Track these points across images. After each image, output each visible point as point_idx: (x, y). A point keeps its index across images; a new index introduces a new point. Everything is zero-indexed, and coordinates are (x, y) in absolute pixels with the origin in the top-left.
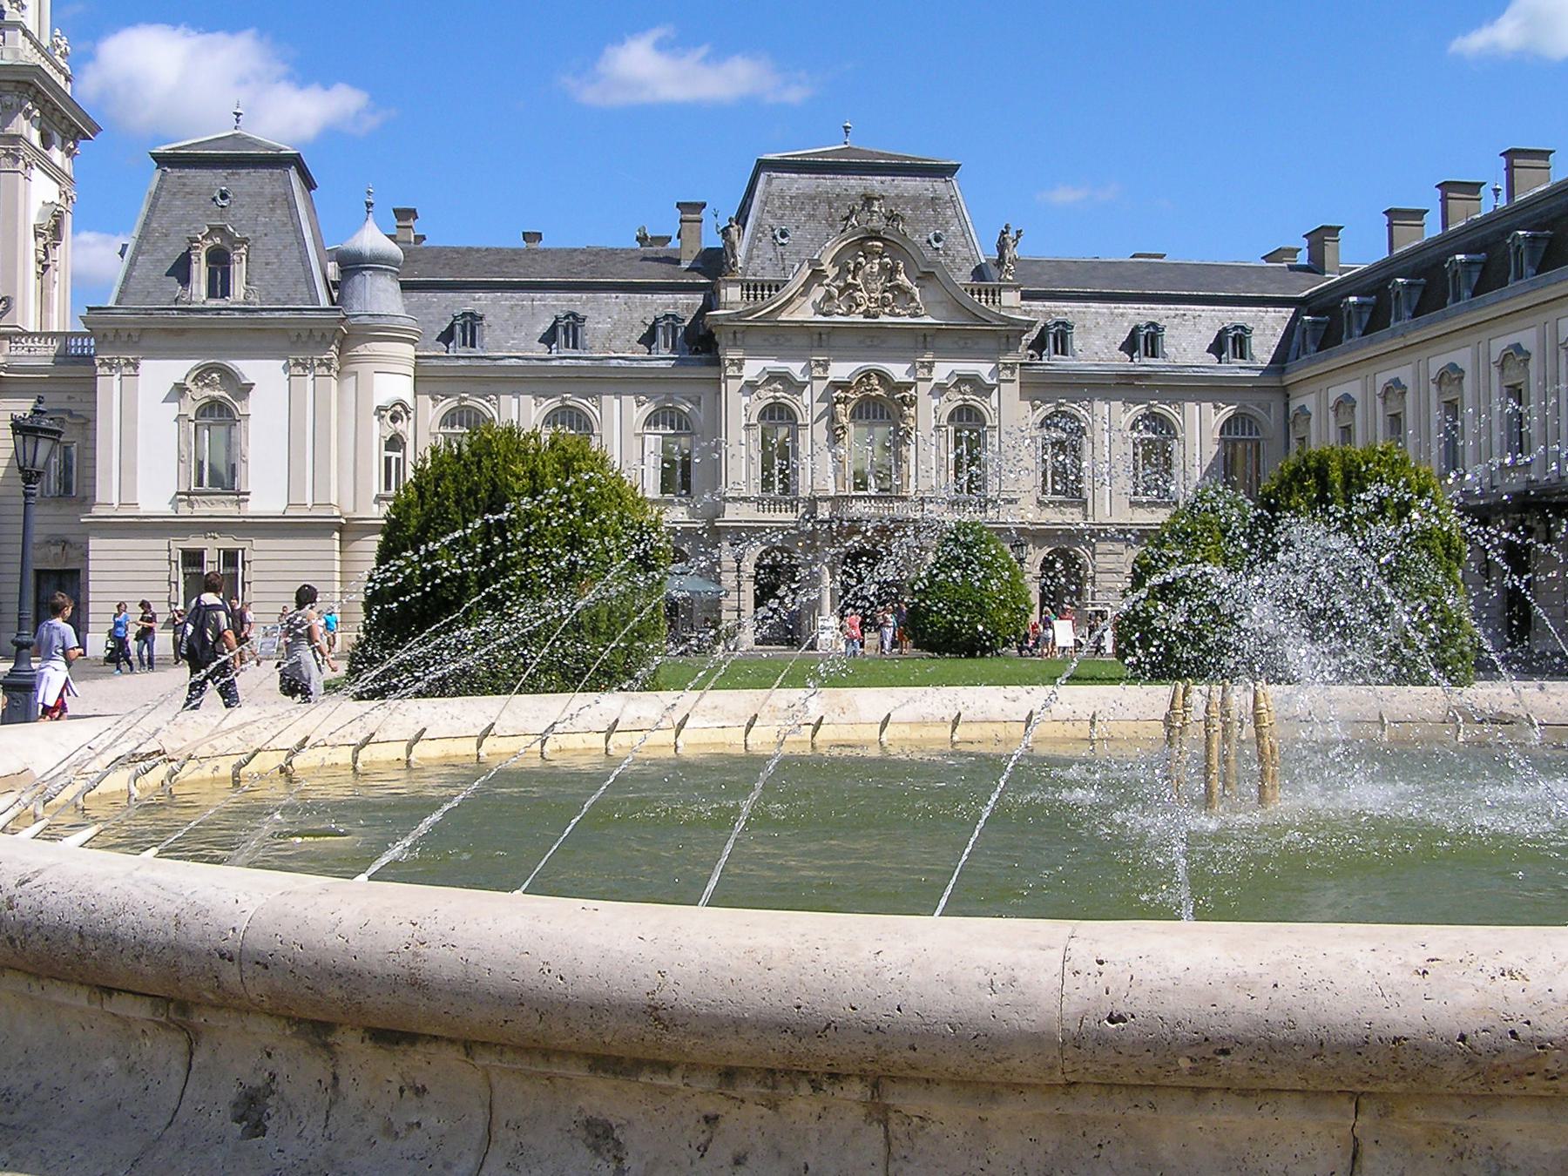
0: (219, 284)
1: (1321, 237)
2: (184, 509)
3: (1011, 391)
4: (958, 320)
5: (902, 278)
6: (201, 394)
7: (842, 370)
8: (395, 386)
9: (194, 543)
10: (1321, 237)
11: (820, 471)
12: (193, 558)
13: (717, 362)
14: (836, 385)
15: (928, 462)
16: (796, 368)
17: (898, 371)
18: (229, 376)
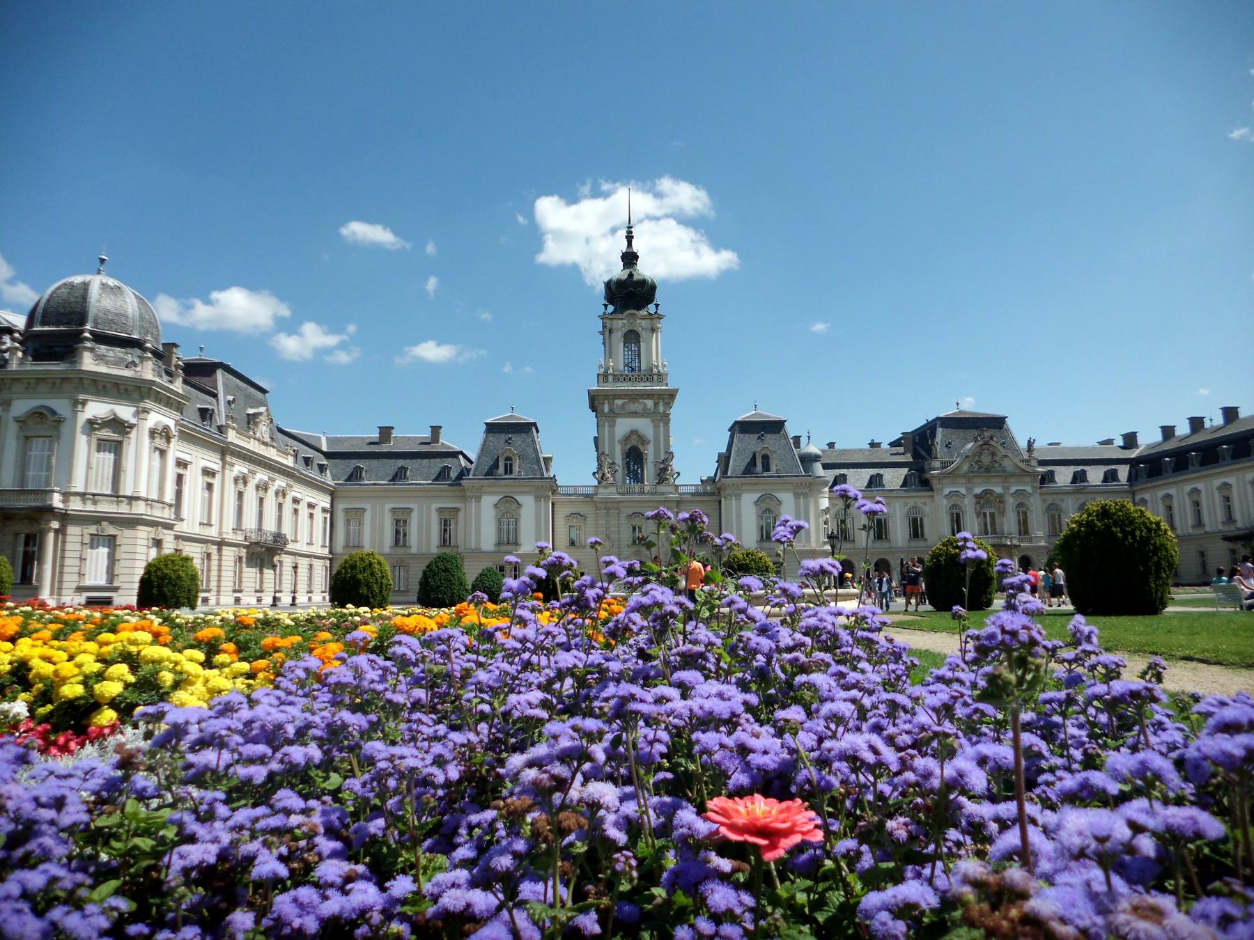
3: (1037, 496)
6: (764, 506)
7: (978, 490)
13: (932, 490)
14: (977, 496)
16: (963, 490)
17: (998, 490)
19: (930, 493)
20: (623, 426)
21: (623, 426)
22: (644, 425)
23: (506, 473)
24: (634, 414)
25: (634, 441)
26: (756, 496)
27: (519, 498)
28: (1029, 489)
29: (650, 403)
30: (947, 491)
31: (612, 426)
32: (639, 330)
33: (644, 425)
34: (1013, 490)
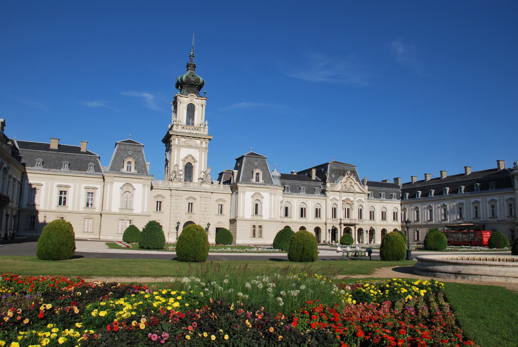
0: (257, 180)
1: (396, 179)
2: (253, 218)
4: (360, 191)
5: (353, 184)
6: (256, 198)
7: (344, 198)
8: (281, 198)
9: (254, 223)
10: (396, 179)
11: (340, 214)
12: (254, 226)
13: (325, 195)
15: (354, 214)
16: (338, 198)
17: (352, 199)
18: (260, 195)
19: (325, 198)
20: (184, 152)
21: (184, 152)
22: (195, 153)
23: (127, 170)
24: (190, 147)
25: (190, 160)
26: (252, 193)
27: (134, 185)
28: (363, 200)
29: (198, 142)
30: (331, 198)
31: (179, 152)
32: (195, 104)
33: (195, 153)
34: (357, 199)
